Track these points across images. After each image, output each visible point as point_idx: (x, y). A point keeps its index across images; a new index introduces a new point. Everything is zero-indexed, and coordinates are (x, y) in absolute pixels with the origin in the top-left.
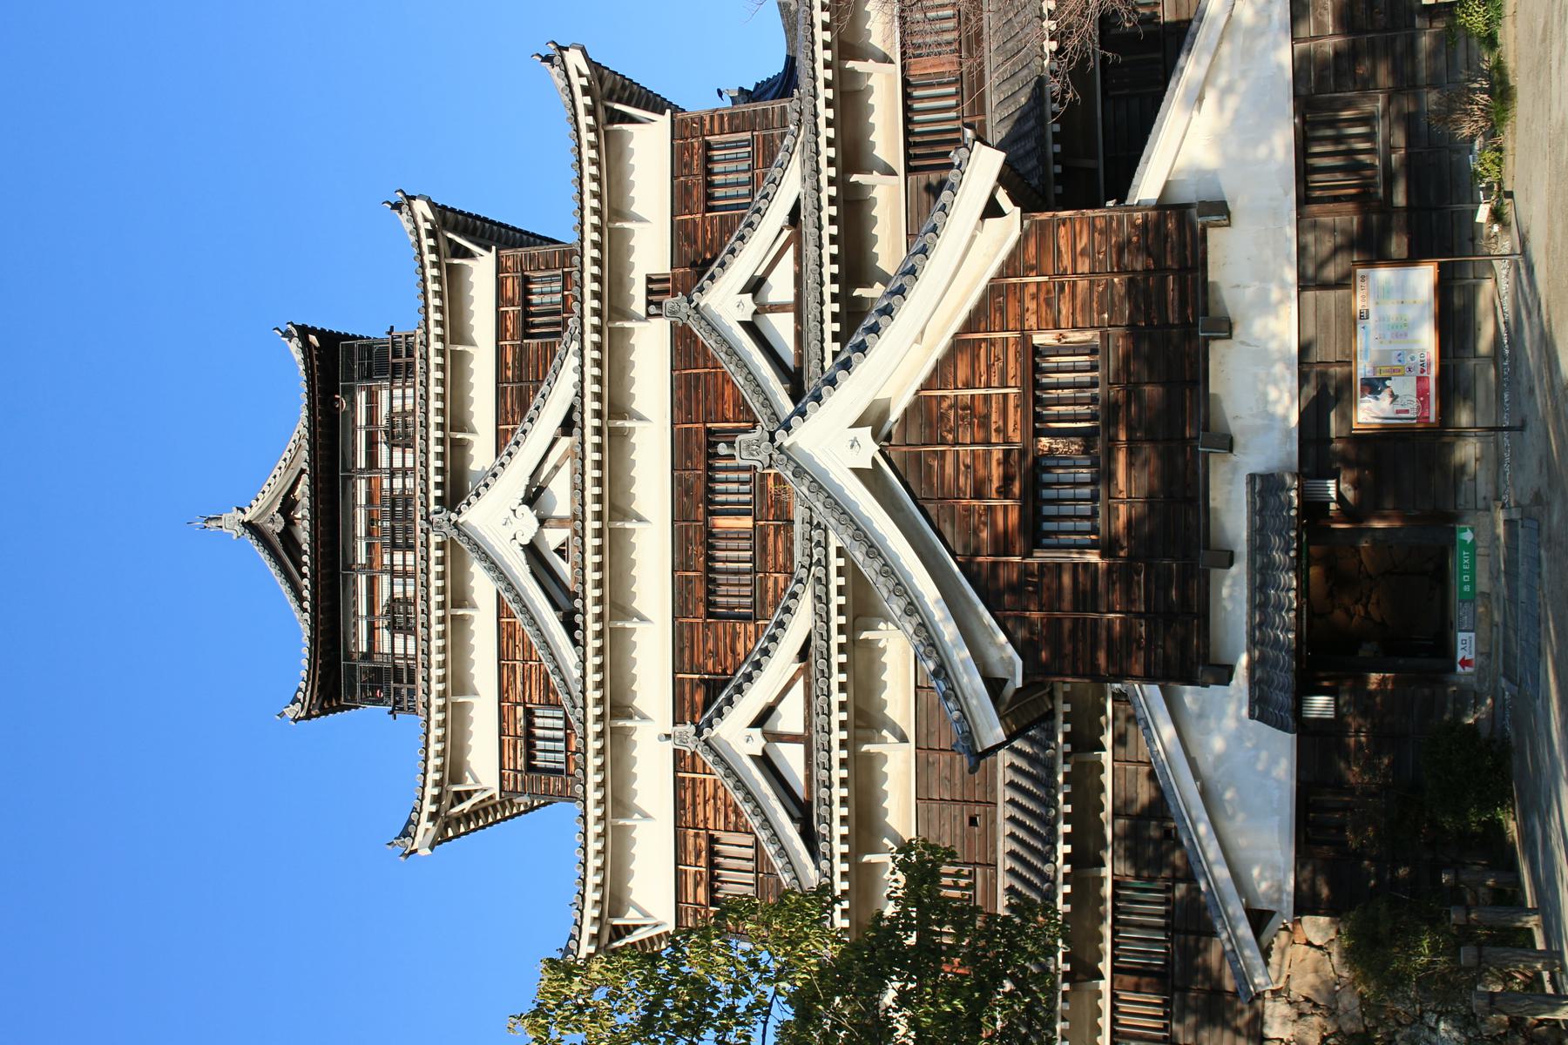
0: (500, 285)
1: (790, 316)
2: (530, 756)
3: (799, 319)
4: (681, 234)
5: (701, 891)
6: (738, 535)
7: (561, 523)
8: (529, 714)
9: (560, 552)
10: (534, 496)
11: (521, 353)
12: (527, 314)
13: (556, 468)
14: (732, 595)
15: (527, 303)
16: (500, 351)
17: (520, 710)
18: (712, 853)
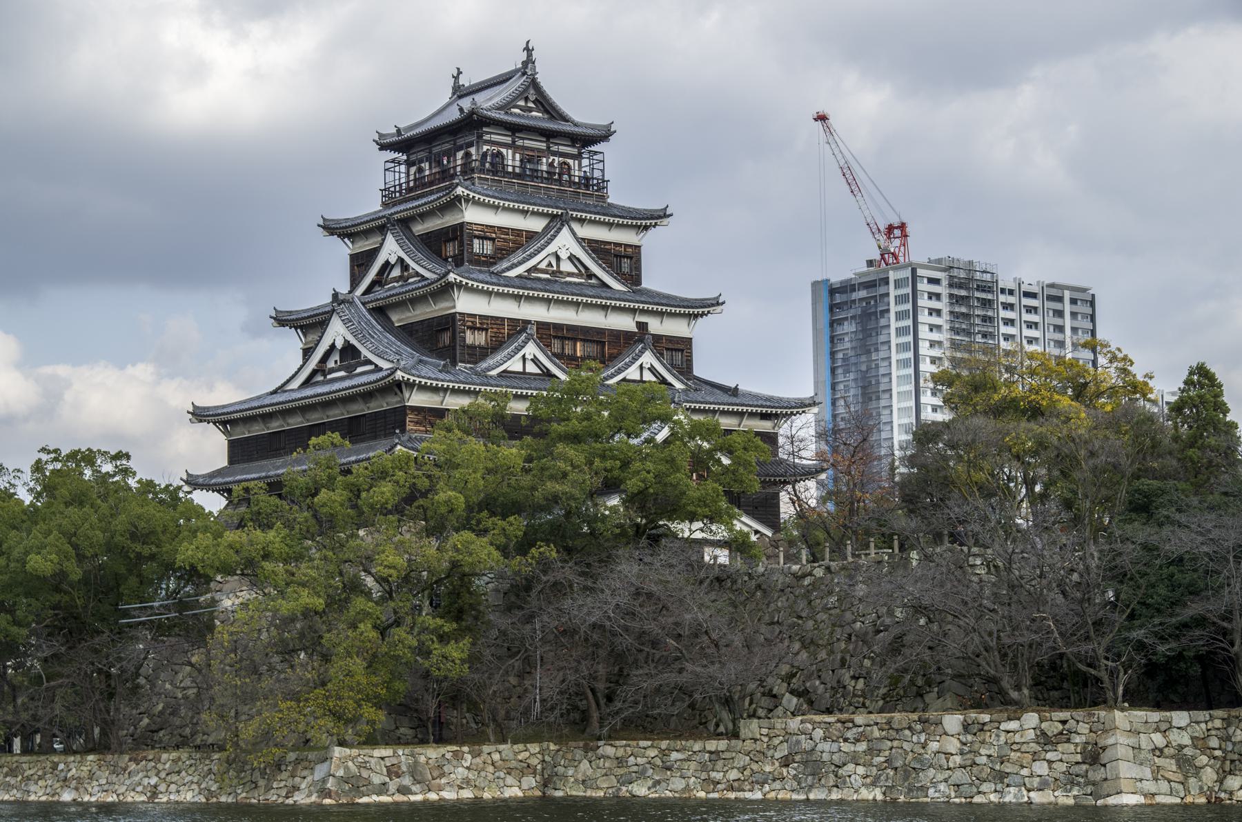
0: (630, 246)
1: (639, 378)
2: (478, 237)
3: (639, 381)
4: (658, 339)
5: (470, 324)
6: (575, 350)
7: (558, 266)
8: (493, 240)
9: (550, 264)
10: (572, 258)
11: (608, 252)
12: (621, 257)
13: (576, 266)
15: (624, 257)
16: (610, 243)
17: (494, 235)
18: (483, 329)
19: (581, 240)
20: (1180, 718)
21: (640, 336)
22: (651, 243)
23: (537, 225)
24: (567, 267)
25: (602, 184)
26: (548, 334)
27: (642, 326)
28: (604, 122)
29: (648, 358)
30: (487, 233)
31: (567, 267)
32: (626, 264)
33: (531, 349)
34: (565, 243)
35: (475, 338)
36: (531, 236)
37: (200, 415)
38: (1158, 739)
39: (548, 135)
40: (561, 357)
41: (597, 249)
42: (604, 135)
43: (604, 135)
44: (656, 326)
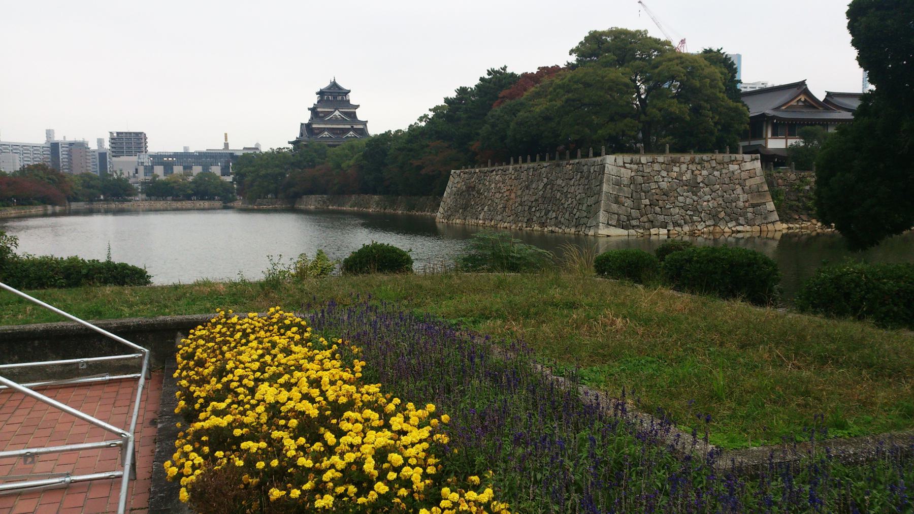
14: (336, 132)
19: (340, 112)
20: (325, 196)
21: (352, 129)
22: (357, 111)
23: (332, 110)
24: (339, 117)
25: (349, 101)
26: (331, 130)
27: (352, 127)
28: (349, 89)
29: (351, 133)
30: (322, 112)
31: (339, 117)
32: (352, 115)
33: (326, 133)
34: (337, 113)
35: (316, 131)
36: (331, 112)
37: (289, 143)
38: (320, 199)
39: (340, 93)
40: (334, 134)
41: (345, 113)
42: (349, 91)
43: (349, 91)
44: (355, 127)
